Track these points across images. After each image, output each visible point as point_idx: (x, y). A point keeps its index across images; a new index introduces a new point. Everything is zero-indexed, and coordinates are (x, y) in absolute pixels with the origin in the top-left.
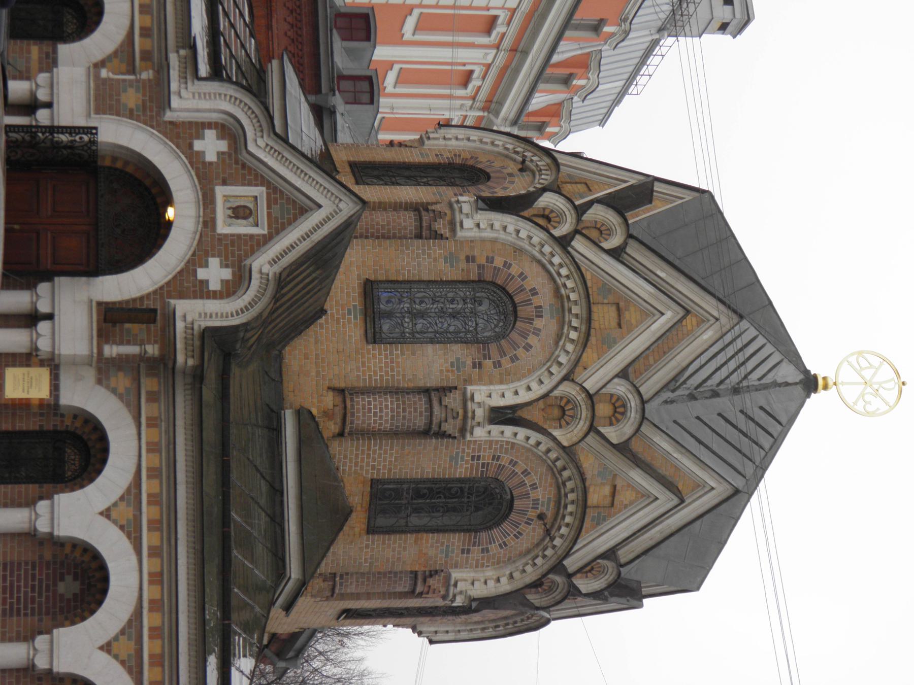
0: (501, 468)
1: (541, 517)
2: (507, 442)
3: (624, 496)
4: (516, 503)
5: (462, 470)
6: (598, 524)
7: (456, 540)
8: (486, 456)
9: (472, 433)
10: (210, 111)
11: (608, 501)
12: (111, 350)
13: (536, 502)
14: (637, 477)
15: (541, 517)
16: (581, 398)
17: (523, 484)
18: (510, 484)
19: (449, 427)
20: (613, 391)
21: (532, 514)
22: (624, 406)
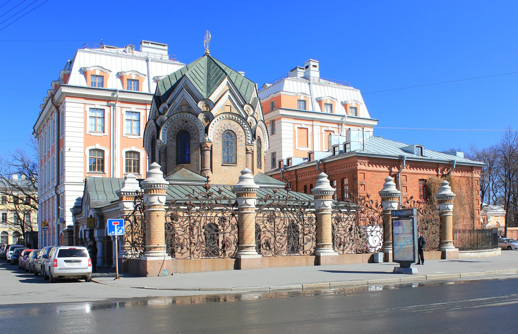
0: (174, 134)
1: (186, 122)
2: (168, 134)
3: (184, 102)
4: (183, 129)
5: (174, 143)
6: (191, 107)
7: (192, 142)
8: (171, 138)
9: (164, 143)
10: (85, 208)
11: (186, 106)
12: (98, 226)
13: (182, 124)
14: (177, 101)
15: (186, 122)
16: (159, 118)
17: (178, 128)
18: (178, 131)
19: (164, 148)
20: (162, 111)
21: (186, 124)
22: (165, 107)
